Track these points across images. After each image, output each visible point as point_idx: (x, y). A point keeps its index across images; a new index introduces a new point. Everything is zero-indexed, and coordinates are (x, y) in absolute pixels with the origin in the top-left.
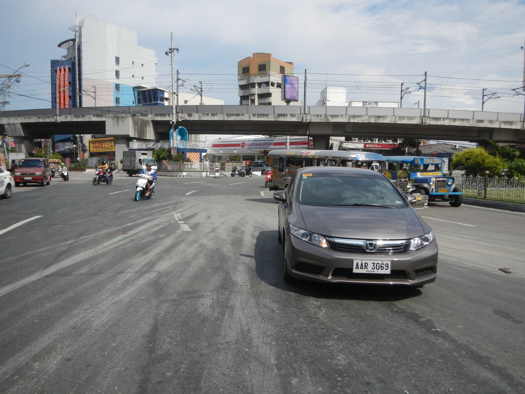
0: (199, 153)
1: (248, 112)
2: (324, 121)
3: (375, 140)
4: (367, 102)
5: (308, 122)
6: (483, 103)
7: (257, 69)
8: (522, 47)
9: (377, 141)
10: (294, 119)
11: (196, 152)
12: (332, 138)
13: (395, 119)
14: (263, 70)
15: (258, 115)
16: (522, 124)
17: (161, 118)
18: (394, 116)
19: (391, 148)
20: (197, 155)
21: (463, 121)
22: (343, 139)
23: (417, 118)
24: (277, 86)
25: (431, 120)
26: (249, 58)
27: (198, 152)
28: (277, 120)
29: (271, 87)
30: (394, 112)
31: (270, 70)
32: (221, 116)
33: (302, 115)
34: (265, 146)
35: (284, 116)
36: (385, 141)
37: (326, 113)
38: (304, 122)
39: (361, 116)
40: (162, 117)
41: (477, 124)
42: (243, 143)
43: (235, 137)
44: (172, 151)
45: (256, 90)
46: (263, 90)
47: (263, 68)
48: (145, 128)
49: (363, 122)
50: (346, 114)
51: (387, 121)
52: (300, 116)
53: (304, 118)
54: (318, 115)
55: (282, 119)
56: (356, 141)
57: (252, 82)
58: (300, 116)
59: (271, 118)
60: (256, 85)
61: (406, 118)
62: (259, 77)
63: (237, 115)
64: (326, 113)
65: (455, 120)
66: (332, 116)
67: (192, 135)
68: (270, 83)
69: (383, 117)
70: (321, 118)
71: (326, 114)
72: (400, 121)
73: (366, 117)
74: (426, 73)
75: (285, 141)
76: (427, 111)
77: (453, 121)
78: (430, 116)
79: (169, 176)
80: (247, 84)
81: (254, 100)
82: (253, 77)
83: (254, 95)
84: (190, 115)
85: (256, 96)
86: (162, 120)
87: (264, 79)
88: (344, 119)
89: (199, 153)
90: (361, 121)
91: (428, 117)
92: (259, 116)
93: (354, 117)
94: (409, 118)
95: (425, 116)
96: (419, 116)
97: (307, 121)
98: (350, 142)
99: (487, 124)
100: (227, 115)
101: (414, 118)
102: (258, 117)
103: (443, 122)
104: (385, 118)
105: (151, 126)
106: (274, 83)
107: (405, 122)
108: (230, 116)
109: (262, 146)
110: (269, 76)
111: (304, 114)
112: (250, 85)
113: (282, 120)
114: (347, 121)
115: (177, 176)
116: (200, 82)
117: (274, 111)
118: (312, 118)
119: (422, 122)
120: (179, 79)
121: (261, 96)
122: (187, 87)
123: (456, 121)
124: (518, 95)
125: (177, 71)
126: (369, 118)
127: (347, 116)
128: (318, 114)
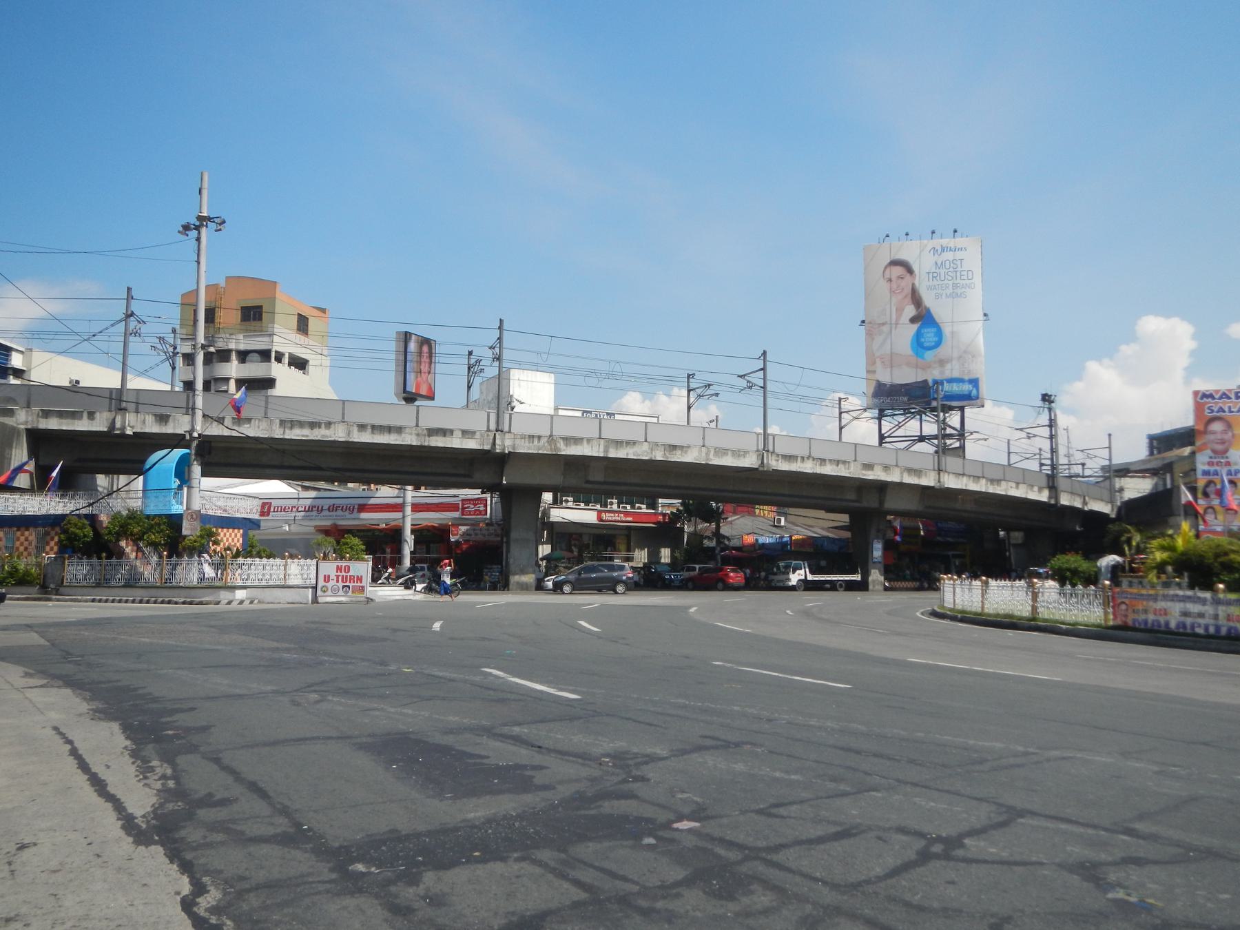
0: (241, 531)
1: (343, 418)
2: (545, 452)
3: (612, 504)
4: (590, 412)
5: (507, 452)
6: (841, 428)
9: (615, 507)
10: (471, 444)
11: (234, 528)
13: (708, 454)
14: (254, 319)
15: (373, 427)
16: (937, 476)
17: (60, 424)
18: (703, 446)
19: (654, 523)
20: (236, 536)
21: (838, 465)
23: (751, 454)
24: (290, 364)
25: (778, 460)
27: (239, 529)
28: (426, 444)
29: (274, 363)
30: (703, 438)
32: (264, 425)
34: (334, 513)
35: (445, 436)
36: (633, 507)
37: (552, 432)
38: (498, 451)
39: (634, 443)
40: (64, 421)
41: (864, 472)
43: (236, 486)
44: (185, 524)
46: (254, 370)
47: (253, 315)
48: (7, 451)
49: (639, 458)
51: (690, 457)
52: (488, 435)
53: (498, 442)
54: (533, 436)
55: (438, 442)
56: (570, 504)
58: (488, 435)
59: (409, 439)
60: (234, 356)
61: (730, 453)
63: (313, 425)
64: (552, 432)
65: (823, 461)
66: (567, 440)
67: (121, 476)
68: (273, 355)
69: (682, 447)
70: (541, 444)
71: (551, 436)
72: (717, 459)
73: (646, 446)
74: (765, 353)
75: (400, 501)
76: (771, 438)
77: (821, 465)
78: (777, 451)
79: (184, 603)
84: (163, 419)
85: (232, 384)
86: (64, 428)
87: (258, 343)
88: (595, 449)
89: (241, 531)
90: (634, 455)
91: (773, 452)
92: (375, 431)
93: (619, 443)
94: (737, 453)
95: (768, 451)
96: (756, 449)
97: (504, 449)
99: (879, 473)
100: (283, 423)
101: (746, 453)
102: (373, 433)
103: (802, 465)
104: (686, 452)
105: (22, 447)
107: (728, 461)
108: (291, 428)
109: (325, 513)
110: (271, 335)
111: (497, 430)
113: (440, 445)
114: (602, 455)
115: (218, 603)
116: (173, 328)
117: (417, 421)
118: (518, 442)
119: (762, 463)
120: (132, 314)
122: (147, 339)
123: (825, 465)
125: (129, 289)
126: (652, 450)
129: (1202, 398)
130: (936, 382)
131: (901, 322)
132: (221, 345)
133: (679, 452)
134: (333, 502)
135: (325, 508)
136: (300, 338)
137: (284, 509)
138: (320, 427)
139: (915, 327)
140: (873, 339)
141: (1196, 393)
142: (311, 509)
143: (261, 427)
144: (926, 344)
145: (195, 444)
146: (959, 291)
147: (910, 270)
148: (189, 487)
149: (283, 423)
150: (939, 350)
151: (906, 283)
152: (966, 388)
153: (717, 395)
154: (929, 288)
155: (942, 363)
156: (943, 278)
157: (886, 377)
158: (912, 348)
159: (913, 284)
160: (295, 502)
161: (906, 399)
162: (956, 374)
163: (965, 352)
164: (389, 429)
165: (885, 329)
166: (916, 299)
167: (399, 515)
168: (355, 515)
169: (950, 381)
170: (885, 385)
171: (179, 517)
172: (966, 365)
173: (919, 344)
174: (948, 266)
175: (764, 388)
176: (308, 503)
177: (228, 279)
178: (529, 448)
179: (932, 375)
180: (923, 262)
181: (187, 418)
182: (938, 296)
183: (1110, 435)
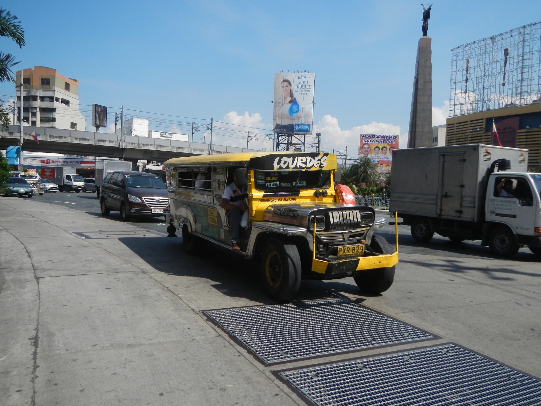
1: (70, 135)
4: (164, 133)
6: (248, 142)
7: (40, 82)
8: (272, 102)
10: (112, 145)
11: (33, 169)
12: (139, 161)
13: (191, 150)
14: (47, 84)
22: (146, 162)
26: (30, 69)
29: (55, 102)
30: (190, 145)
32: (44, 137)
33: (119, 142)
35: (103, 142)
39: (166, 146)
46: (47, 104)
47: (46, 82)
50: (155, 144)
53: (121, 145)
54: (132, 143)
55: (101, 144)
56: (155, 164)
59: (92, 143)
60: (38, 98)
62: (41, 91)
63: (60, 137)
66: (144, 145)
69: (182, 148)
70: (135, 145)
71: (138, 143)
73: (170, 147)
74: (212, 119)
75: (94, 161)
76: (213, 146)
80: (27, 96)
83: (36, 108)
84: (11, 134)
85: (38, 110)
88: (153, 147)
91: (214, 150)
93: (161, 146)
98: (150, 164)
100: (50, 136)
101: (204, 150)
104: (184, 149)
106: (59, 99)
108: (53, 138)
110: (54, 91)
112: (30, 98)
117: (94, 137)
121: (43, 110)
124: (269, 139)
127: (155, 145)
128: (132, 142)
129: (363, 137)
130: (296, 125)
131: (286, 103)
132: (33, 94)
133: (181, 149)
134: (71, 160)
136: (66, 92)
137: (55, 162)
138: (62, 138)
139: (290, 105)
140: (276, 108)
141: (361, 135)
143: (43, 137)
144: (294, 111)
145: (21, 146)
146: (306, 93)
147: (290, 84)
148: (20, 158)
150: (298, 113)
151: (288, 89)
152: (306, 127)
153: (200, 130)
154: (296, 91)
155: (299, 118)
156: (301, 88)
157: (280, 123)
158: (289, 112)
159: (291, 89)
160: (57, 160)
161: (286, 130)
162: (303, 122)
163: (306, 115)
164: (85, 139)
165: (280, 105)
166: (291, 95)
167: (94, 165)
168: (79, 164)
169: (301, 125)
170: (279, 125)
171: (17, 165)
172: (307, 119)
173: (291, 111)
174: (303, 83)
175: (211, 129)
176: (63, 160)
177: (36, 67)
178: (131, 147)
179: (295, 122)
180: (295, 82)
181: (19, 134)
182: (298, 94)
183: (346, 147)
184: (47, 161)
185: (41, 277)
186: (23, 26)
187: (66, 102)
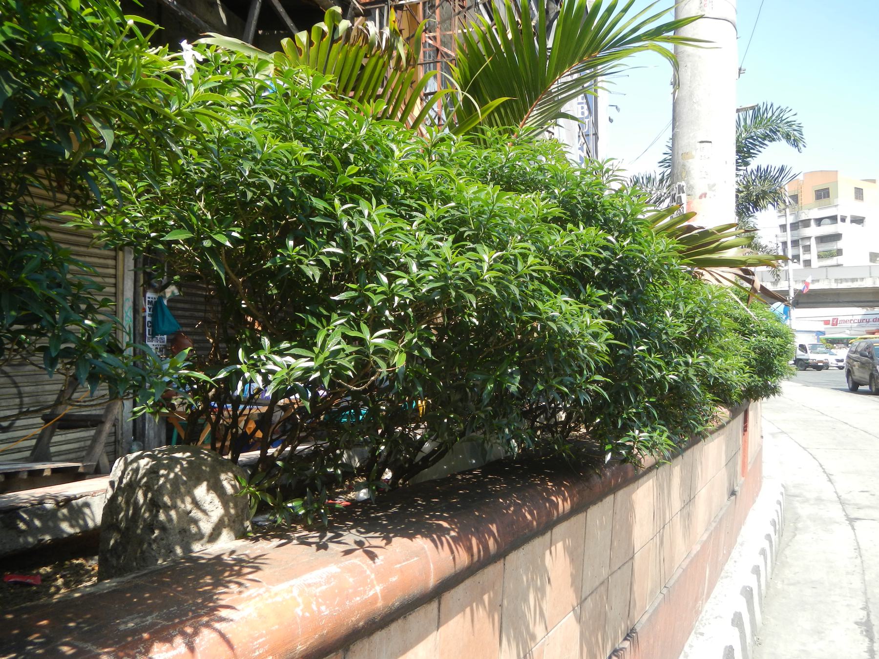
1: (870, 274)
7: (813, 196)
14: (824, 198)
31: (837, 197)
32: (826, 282)
42: (833, 319)
45: (813, 231)
46: (827, 229)
47: (823, 194)
57: (804, 218)
63: (853, 280)
81: (810, 246)
82: (806, 211)
100: (836, 280)
112: (800, 224)
121: (822, 239)
132: (803, 217)
134: (874, 316)
135: (871, 320)
142: (862, 321)
149: (836, 280)
160: (850, 318)
176: (860, 317)
184: (833, 321)
185: (857, 519)
186: (798, 119)
187: (858, 220)
